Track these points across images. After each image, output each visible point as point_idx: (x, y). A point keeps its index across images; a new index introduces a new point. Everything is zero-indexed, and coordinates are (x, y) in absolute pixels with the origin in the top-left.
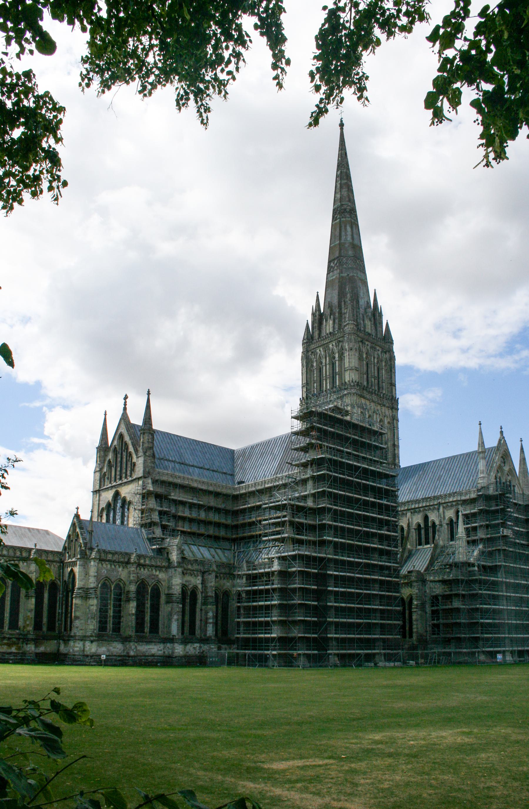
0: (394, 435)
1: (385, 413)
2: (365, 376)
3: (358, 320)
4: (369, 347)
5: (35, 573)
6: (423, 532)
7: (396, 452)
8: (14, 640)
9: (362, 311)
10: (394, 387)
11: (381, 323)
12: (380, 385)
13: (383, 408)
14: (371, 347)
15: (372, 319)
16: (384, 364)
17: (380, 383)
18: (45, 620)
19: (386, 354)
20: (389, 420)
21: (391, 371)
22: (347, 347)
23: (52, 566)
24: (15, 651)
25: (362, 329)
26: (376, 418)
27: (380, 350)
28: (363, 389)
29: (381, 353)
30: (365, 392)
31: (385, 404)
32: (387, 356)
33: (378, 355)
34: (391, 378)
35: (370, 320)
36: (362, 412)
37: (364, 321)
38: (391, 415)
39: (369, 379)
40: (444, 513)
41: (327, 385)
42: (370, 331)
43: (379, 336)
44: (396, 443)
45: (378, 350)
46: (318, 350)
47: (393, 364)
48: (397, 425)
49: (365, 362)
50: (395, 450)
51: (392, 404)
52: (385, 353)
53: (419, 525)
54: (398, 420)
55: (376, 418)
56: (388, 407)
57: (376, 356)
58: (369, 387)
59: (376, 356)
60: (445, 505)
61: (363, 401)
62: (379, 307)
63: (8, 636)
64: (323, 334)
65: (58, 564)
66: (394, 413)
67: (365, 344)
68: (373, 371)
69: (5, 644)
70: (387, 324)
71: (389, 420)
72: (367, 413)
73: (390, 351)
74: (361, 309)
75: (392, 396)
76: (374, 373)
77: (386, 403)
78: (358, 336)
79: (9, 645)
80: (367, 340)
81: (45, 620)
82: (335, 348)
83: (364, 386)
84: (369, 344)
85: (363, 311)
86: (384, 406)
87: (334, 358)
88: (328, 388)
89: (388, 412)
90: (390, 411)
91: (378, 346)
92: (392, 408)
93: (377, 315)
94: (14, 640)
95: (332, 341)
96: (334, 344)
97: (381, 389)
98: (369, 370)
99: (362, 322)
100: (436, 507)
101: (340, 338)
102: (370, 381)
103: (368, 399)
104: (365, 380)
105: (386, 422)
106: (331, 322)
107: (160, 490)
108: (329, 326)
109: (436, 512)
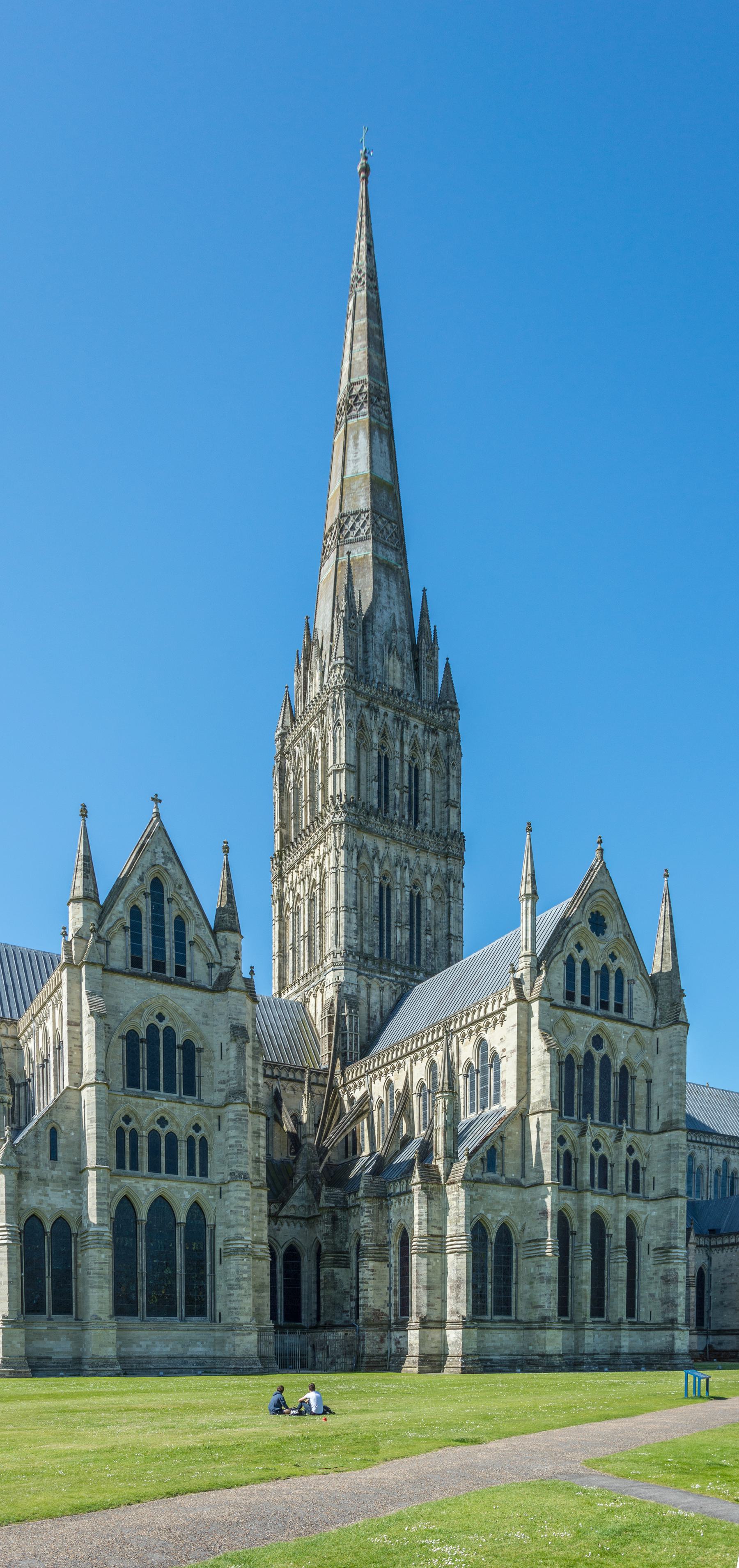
2: (375, 785)
11: (434, 668)
19: (437, 734)
27: (421, 727)
29: (424, 731)
33: (414, 736)
39: (390, 793)
52: (434, 732)
59: (407, 739)
68: (398, 772)
73: (451, 728)
76: (402, 777)
83: (372, 807)
91: (415, 716)
98: (390, 771)
102: (391, 797)
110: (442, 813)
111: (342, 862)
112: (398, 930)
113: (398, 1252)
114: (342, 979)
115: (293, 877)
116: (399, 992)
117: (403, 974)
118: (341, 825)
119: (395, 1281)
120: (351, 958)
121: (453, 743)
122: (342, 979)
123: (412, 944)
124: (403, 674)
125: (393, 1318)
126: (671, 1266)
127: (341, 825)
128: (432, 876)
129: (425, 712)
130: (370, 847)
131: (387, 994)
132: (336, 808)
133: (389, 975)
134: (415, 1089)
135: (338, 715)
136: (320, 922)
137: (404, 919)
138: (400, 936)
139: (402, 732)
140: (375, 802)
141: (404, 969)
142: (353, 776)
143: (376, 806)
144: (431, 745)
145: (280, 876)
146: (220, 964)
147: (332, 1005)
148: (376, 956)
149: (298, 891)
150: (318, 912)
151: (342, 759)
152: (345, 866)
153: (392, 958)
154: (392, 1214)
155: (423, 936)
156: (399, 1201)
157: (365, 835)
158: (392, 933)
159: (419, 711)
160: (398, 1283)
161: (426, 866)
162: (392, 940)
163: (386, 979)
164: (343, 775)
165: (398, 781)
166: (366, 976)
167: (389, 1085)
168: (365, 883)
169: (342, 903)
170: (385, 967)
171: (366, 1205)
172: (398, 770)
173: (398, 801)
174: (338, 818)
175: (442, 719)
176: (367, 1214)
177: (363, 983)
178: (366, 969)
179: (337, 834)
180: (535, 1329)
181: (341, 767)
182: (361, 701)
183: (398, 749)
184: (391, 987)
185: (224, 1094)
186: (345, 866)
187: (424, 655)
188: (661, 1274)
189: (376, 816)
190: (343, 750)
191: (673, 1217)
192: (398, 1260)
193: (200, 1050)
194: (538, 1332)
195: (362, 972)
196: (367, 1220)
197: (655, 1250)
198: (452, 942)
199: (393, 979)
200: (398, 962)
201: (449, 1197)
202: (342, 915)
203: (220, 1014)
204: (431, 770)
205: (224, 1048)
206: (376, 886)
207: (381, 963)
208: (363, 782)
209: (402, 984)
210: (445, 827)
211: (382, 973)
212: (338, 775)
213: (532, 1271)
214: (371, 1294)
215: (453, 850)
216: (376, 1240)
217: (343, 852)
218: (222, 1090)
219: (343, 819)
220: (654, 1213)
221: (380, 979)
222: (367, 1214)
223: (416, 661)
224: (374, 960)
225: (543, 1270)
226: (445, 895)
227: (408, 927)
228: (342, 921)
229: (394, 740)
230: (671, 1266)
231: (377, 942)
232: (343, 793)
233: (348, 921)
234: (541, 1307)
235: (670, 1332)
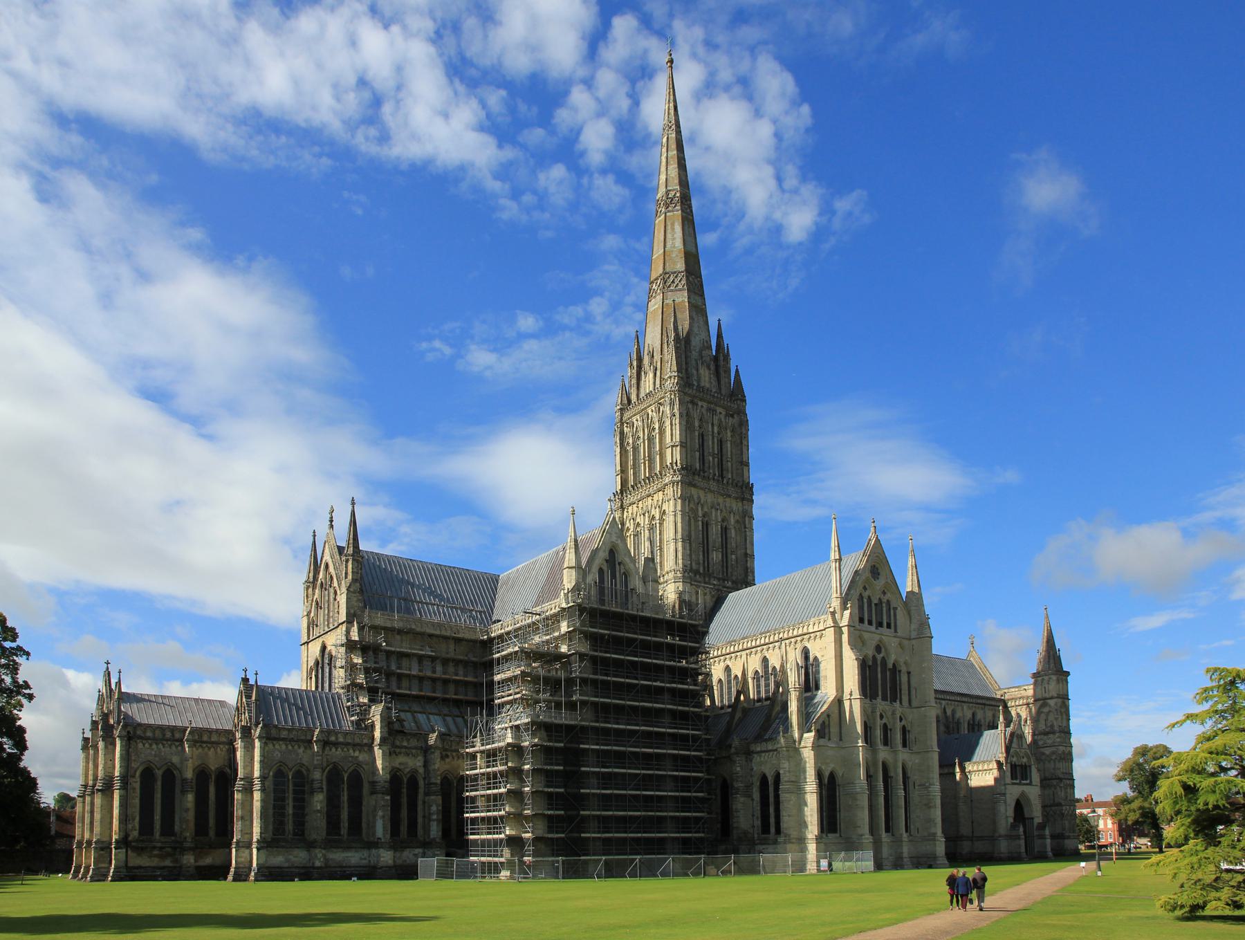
0: (746, 540)
1: (730, 507)
2: (697, 454)
3: (689, 369)
4: (704, 411)
5: (191, 760)
7: (749, 565)
8: (169, 850)
9: (694, 354)
10: (745, 469)
11: (728, 371)
12: (724, 466)
13: (728, 500)
14: (709, 410)
15: (712, 367)
16: (729, 434)
17: (724, 463)
18: (212, 822)
20: (737, 517)
21: (741, 443)
22: (668, 412)
23: (219, 749)
24: (171, 865)
25: (695, 383)
26: (716, 516)
27: (724, 413)
28: (694, 474)
30: (696, 477)
31: (730, 493)
32: (736, 420)
33: (720, 420)
34: (742, 454)
35: (709, 368)
36: (691, 509)
37: (697, 370)
38: (741, 509)
41: (644, 472)
42: (707, 385)
43: (723, 392)
44: (748, 552)
45: (720, 413)
46: (635, 420)
47: (744, 432)
48: (751, 524)
49: (697, 434)
50: (747, 561)
51: (743, 493)
52: (732, 416)
54: (752, 517)
55: (716, 516)
56: (736, 498)
57: (716, 422)
58: (706, 469)
59: (716, 422)
61: (694, 491)
62: (726, 346)
63: (159, 845)
64: (642, 395)
65: (227, 747)
66: (746, 507)
67: (697, 405)
68: (711, 445)
69: (156, 856)
70: (737, 371)
71: (737, 517)
72: (700, 509)
73: (741, 413)
74: (693, 352)
75: (743, 481)
76: (713, 448)
77: (731, 490)
78: (685, 394)
79: (162, 857)
80: (701, 400)
81: (212, 822)
82: (654, 414)
83: (696, 469)
84: (705, 405)
85: (697, 354)
86: (729, 496)
87: (654, 429)
88: (647, 476)
89: (736, 505)
90: (740, 504)
91: (719, 406)
92: (743, 499)
93: (722, 358)
94: (169, 850)
95: (651, 405)
96: (653, 409)
97: (724, 472)
98: (705, 444)
99: (695, 372)
101: (661, 399)
102: (706, 461)
103: (702, 489)
104: (698, 460)
105: (732, 521)
106: (651, 375)
107: (369, 638)
108: (648, 383)
110: (737, 469)
111: (679, 508)
112: (714, 552)
114: (681, 589)
115: (632, 510)
116: (716, 596)
117: (718, 583)
118: (678, 483)
120: (686, 574)
121: (744, 423)
122: (681, 589)
123: (723, 561)
124: (711, 378)
127: (678, 483)
128: (734, 514)
129: (725, 403)
130: (695, 497)
131: (708, 597)
132: (675, 471)
133: (710, 584)
134: (750, 675)
135: (673, 409)
136: (659, 546)
137: (717, 545)
138: (716, 556)
139: (713, 418)
140: (698, 465)
141: (719, 579)
142: (684, 449)
143: (698, 468)
144: (730, 424)
145: (622, 508)
147: (674, 606)
148: (701, 571)
149: (638, 520)
150: (658, 539)
151: (677, 438)
152: (681, 511)
153: (711, 571)
155: (729, 555)
157: (692, 488)
158: (710, 554)
159: (722, 402)
161: (730, 507)
162: (710, 559)
163: (707, 587)
164: (678, 448)
165: (711, 451)
166: (696, 585)
167: (728, 669)
168: (692, 520)
169: (679, 535)
170: (707, 579)
172: (710, 443)
173: (711, 464)
174: (675, 478)
175: (736, 407)
177: (694, 591)
178: (695, 581)
179: (675, 488)
181: (677, 444)
182: (687, 399)
183: (710, 430)
184: (711, 593)
186: (681, 511)
187: (722, 363)
189: (699, 476)
190: (678, 432)
195: (693, 583)
198: (749, 559)
199: (712, 587)
200: (715, 575)
202: (680, 544)
204: (731, 441)
206: (700, 523)
207: (704, 577)
208: (689, 452)
209: (718, 590)
210: (741, 480)
211: (705, 583)
212: (674, 448)
215: (747, 496)
217: (679, 501)
219: (679, 478)
220: (917, 761)
221: (704, 587)
223: (717, 367)
224: (700, 574)
226: (743, 527)
227: (720, 550)
228: (680, 548)
229: (708, 423)
231: (701, 562)
232: (679, 462)
233: (684, 548)
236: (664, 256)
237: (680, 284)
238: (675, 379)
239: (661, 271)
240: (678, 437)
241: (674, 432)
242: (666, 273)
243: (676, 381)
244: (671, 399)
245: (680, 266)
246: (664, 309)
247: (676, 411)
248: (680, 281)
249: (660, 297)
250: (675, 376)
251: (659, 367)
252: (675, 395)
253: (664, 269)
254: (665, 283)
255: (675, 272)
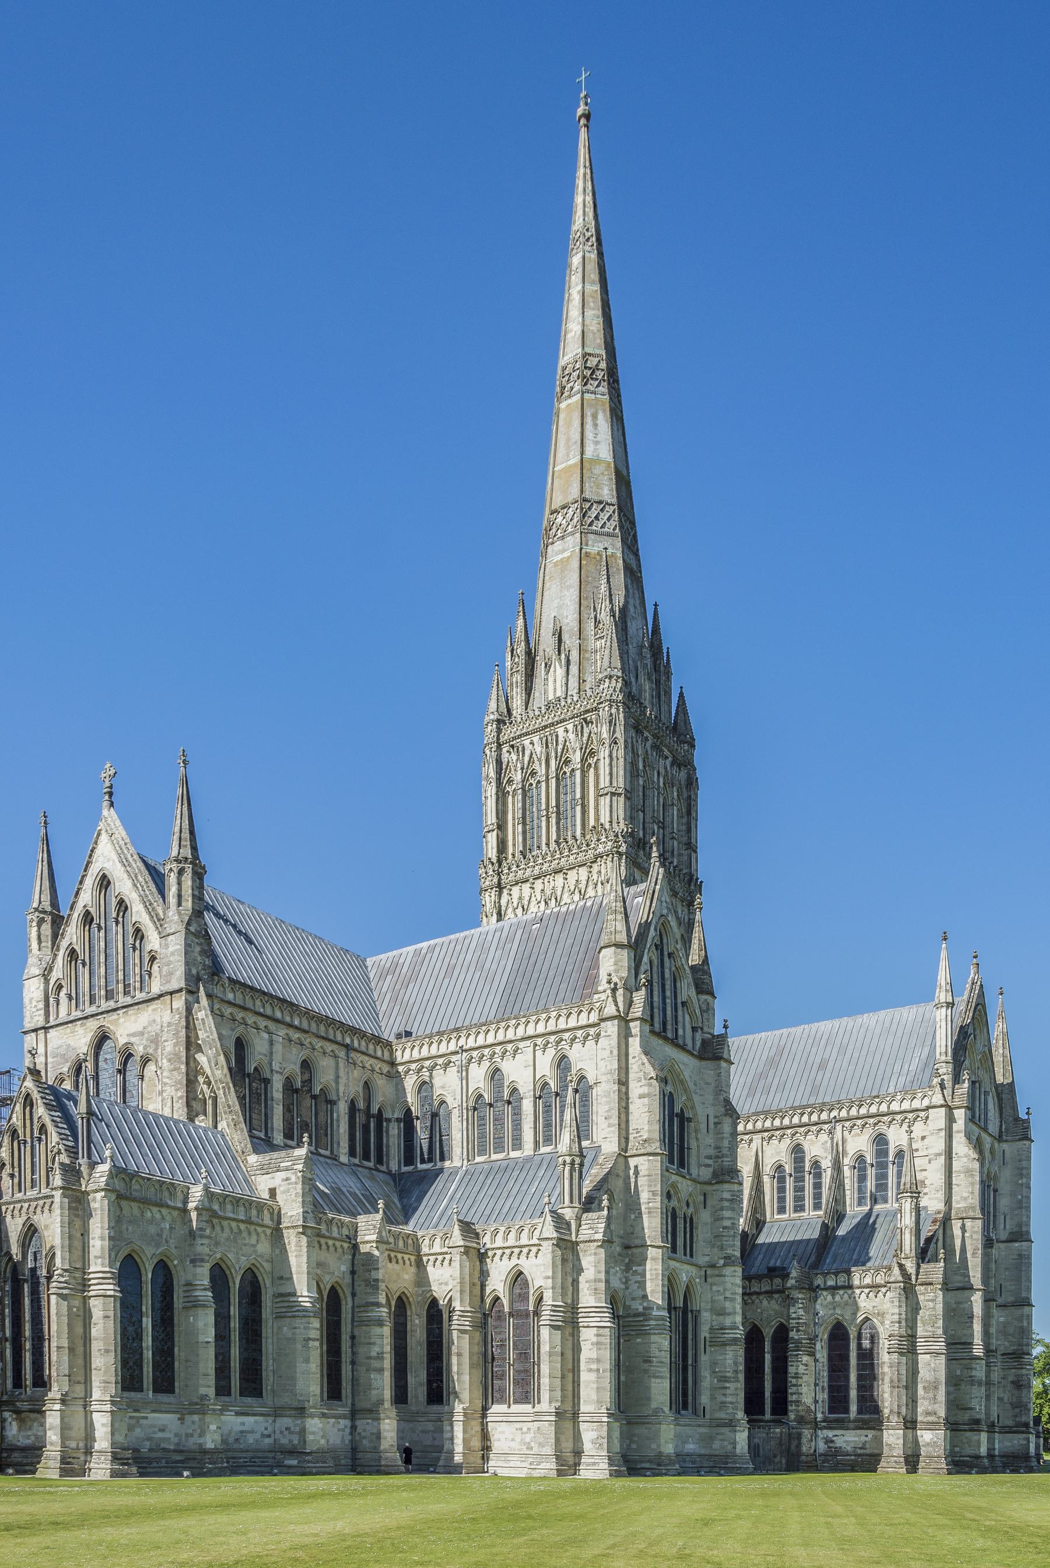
6: (790, 1183)
40: (844, 1141)
53: (780, 1168)
60: (847, 1124)
100: (825, 1127)
109: (824, 1137)
113: (825, 1346)
119: (823, 1376)
125: (820, 1416)
126: (1024, 1372)
146: (702, 1029)
154: (818, 1307)
156: (833, 1295)
160: (826, 1380)
171: (800, 1296)
176: (801, 1306)
180: (965, 1430)
185: (711, 1170)
188: (1011, 1379)
191: (1025, 1324)
192: (826, 1356)
193: (689, 1120)
194: (968, 1434)
196: (801, 1312)
197: (1003, 1355)
201: (921, 1298)
203: (707, 1083)
205: (712, 1120)
213: (958, 1373)
214: (804, 1389)
216: (808, 1334)
218: (709, 1166)
222: (801, 1306)
225: (974, 1373)
230: (1024, 1372)
234: (971, 1409)
235: (1024, 1435)
236: (582, 469)
237: (608, 524)
238: (617, 682)
239: (574, 492)
240: (621, 780)
241: (615, 770)
242: (585, 500)
243: (619, 685)
244: (611, 715)
245: (607, 492)
246: (584, 562)
247: (620, 734)
248: (609, 519)
249: (572, 542)
250: (618, 677)
251: (574, 656)
252: (618, 710)
253: (582, 492)
254: (584, 516)
255: (600, 502)
